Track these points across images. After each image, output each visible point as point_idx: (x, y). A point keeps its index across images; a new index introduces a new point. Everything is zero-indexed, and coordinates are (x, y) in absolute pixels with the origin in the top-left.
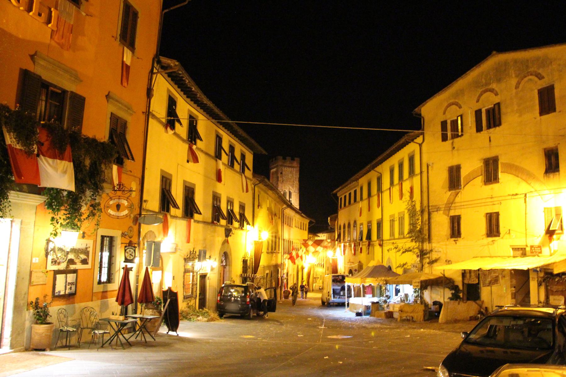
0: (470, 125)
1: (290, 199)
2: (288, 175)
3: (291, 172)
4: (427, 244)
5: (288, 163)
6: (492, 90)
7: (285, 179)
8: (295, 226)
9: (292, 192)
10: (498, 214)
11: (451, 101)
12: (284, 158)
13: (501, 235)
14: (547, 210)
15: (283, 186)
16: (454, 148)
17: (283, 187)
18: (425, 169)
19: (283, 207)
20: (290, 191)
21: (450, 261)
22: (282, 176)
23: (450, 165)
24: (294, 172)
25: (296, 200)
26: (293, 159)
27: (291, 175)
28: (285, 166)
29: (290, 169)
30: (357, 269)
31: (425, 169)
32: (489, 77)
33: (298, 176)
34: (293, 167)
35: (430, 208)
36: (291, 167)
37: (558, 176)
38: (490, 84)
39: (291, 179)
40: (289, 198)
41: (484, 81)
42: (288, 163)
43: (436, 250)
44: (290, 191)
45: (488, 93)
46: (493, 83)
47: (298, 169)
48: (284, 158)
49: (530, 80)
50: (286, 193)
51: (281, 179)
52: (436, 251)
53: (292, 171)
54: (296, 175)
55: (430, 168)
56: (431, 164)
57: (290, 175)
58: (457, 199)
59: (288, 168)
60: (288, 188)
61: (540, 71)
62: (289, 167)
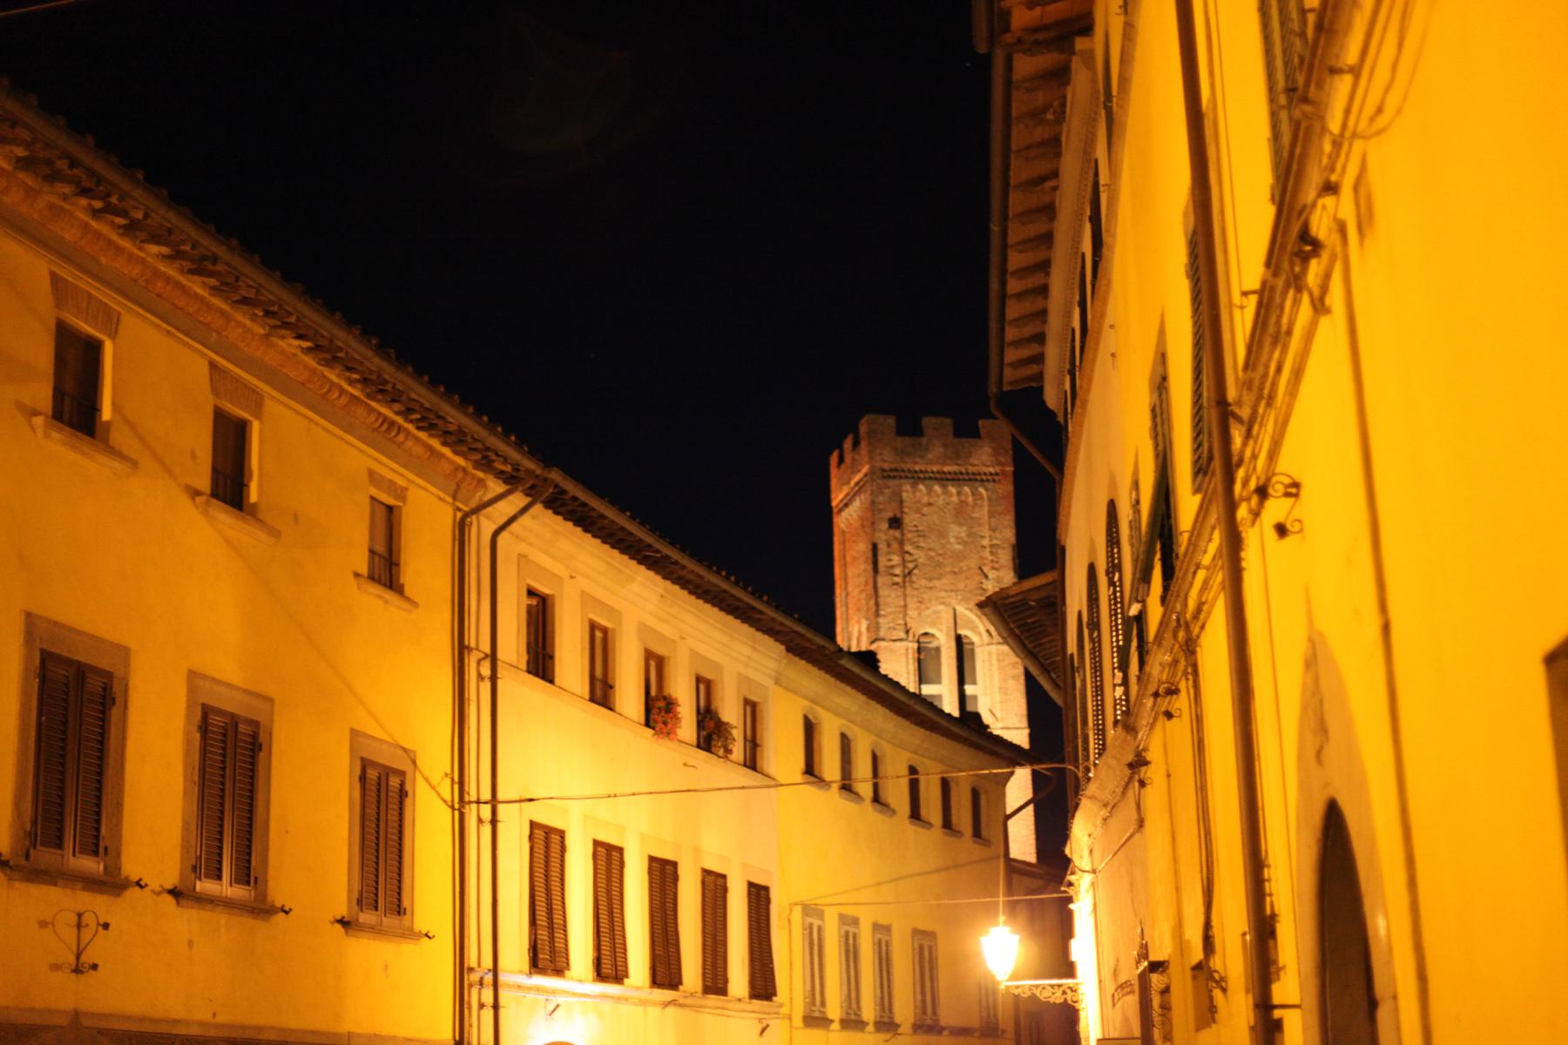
1: (969, 689)
2: (942, 534)
3: (960, 512)
5: (937, 451)
7: (920, 556)
8: (810, 769)
9: (975, 638)
12: (910, 428)
15: (912, 603)
17: (912, 613)
20: (959, 640)
22: (901, 543)
24: (983, 513)
25: (1003, 690)
26: (967, 430)
27: (963, 533)
28: (916, 478)
29: (953, 490)
33: (1008, 534)
34: (972, 479)
36: (956, 479)
39: (959, 557)
40: (961, 682)
42: (937, 451)
44: (959, 640)
47: (1006, 488)
48: (910, 428)
50: (938, 650)
51: (896, 559)
53: (962, 502)
54: (993, 530)
57: (956, 531)
59: (937, 488)
60: (946, 615)
62: (943, 479)
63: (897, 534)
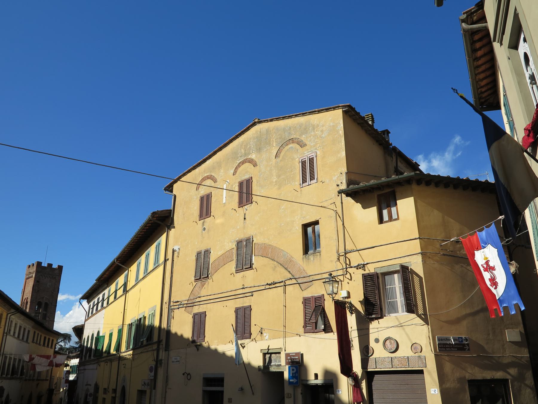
0: (224, 201)
4: (164, 352)
6: (251, 161)
10: (250, 308)
11: (206, 175)
13: (252, 337)
14: (306, 301)
16: (204, 229)
18: (170, 256)
19: (8, 313)
21: (189, 374)
23: (198, 250)
30: (93, 393)
31: (170, 256)
32: (249, 147)
35: (172, 304)
37: (318, 257)
38: (249, 154)
41: (243, 151)
43: (173, 360)
45: (247, 165)
46: (253, 153)
49: (292, 147)
51: (37, 288)
52: (173, 362)
55: (176, 254)
56: (177, 250)
58: (203, 292)
61: (303, 138)
63: (38, 283)
